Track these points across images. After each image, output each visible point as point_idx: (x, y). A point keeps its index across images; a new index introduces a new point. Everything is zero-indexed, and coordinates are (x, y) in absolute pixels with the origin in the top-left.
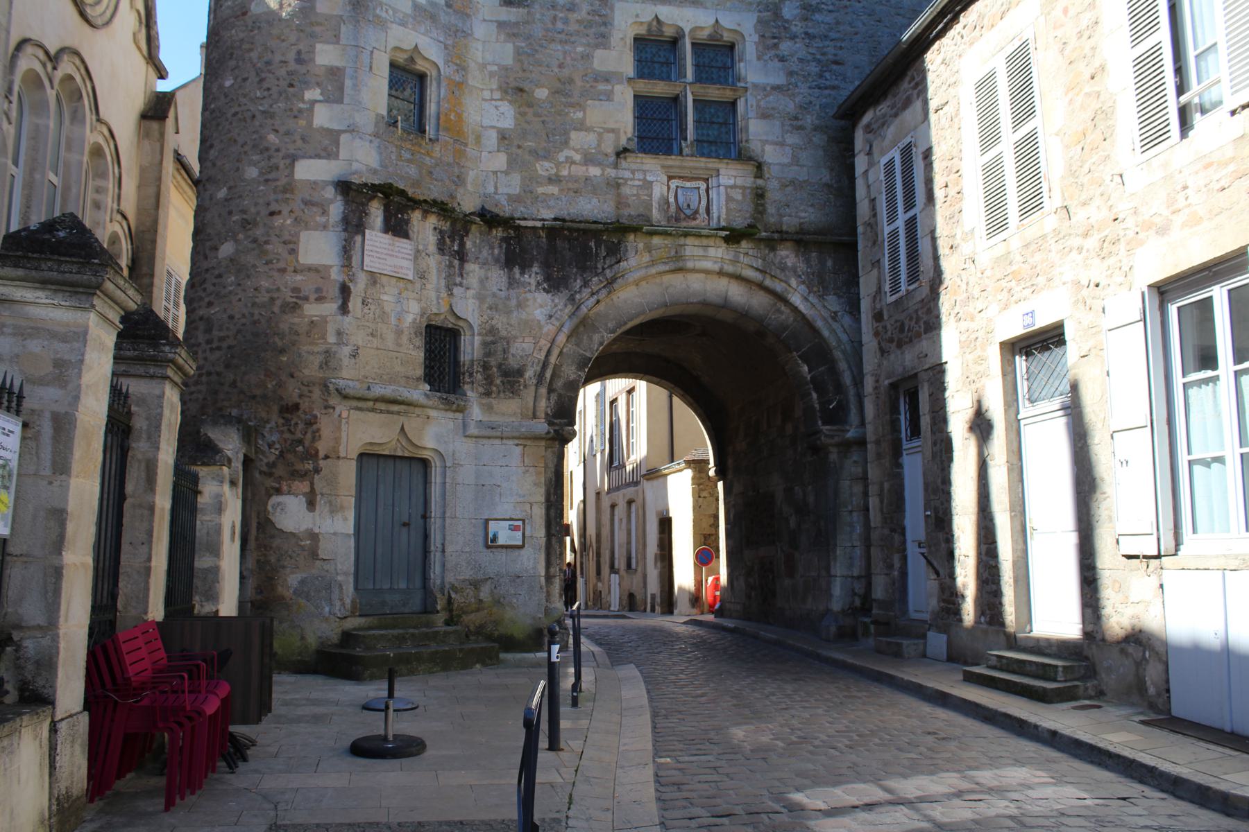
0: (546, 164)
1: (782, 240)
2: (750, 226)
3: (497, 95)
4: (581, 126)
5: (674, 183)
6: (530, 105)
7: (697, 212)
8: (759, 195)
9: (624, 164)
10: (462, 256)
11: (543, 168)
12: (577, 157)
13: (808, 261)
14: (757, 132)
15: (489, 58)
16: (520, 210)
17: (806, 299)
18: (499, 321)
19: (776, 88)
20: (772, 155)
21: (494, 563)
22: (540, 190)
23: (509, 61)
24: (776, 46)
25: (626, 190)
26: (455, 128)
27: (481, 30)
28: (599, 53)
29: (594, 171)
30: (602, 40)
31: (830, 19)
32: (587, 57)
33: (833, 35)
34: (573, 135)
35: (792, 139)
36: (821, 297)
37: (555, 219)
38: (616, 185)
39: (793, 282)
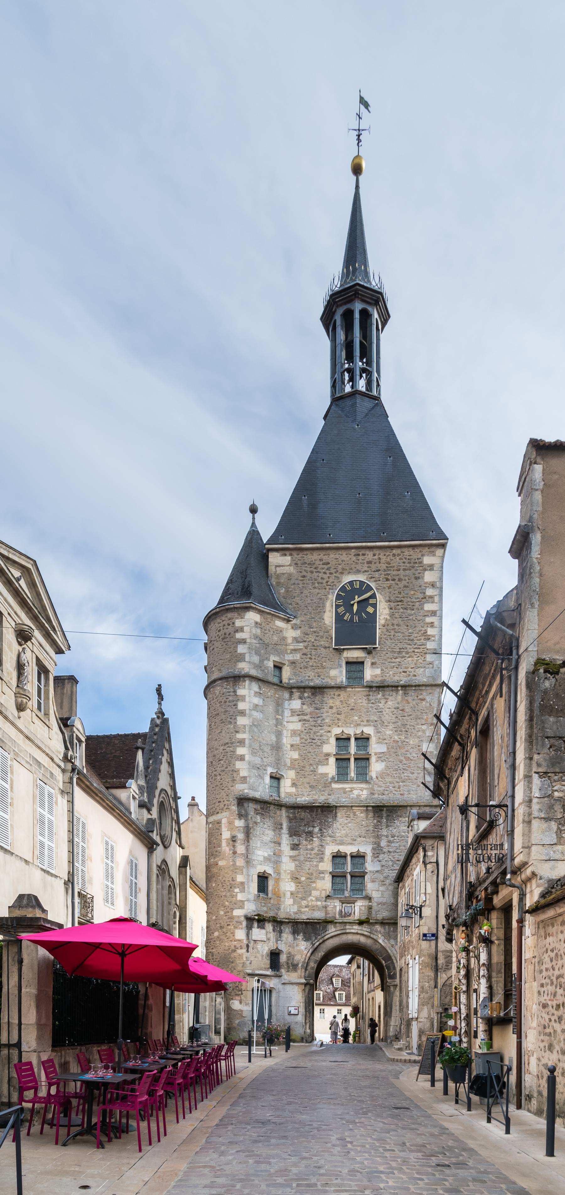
0: (305, 902)
1: (376, 923)
2: (367, 918)
3: (290, 880)
4: (315, 889)
5: (344, 905)
6: (300, 883)
7: (351, 914)
8: (370, 908)
9: (328, 900)
10: (281, 932)
11: (304, 903)
12: (314, 899)
13: (385, 929)
14: (370, 887)
15: (287, 868)
16: (297, 916)
17: (383, 941)
18: (291, 950)
19: (377, 871)
20: (375, 895)
21: (289, 1019)
22: (303, 910)
23: (293, 869)
24: (378, 857)
25: (329, 909)
26: (278, 896)
27: (285, 859)
28: (321, 864)
29: (319, 903)
30: (322, 860)
31: (397, 845)
32: (317, 866)
33: (398, 851)
34: (313, 892)
35: (382, 888)
36: (389, 940)
37: (308, 919)
38: (325, 907)
39: (380, 936)
